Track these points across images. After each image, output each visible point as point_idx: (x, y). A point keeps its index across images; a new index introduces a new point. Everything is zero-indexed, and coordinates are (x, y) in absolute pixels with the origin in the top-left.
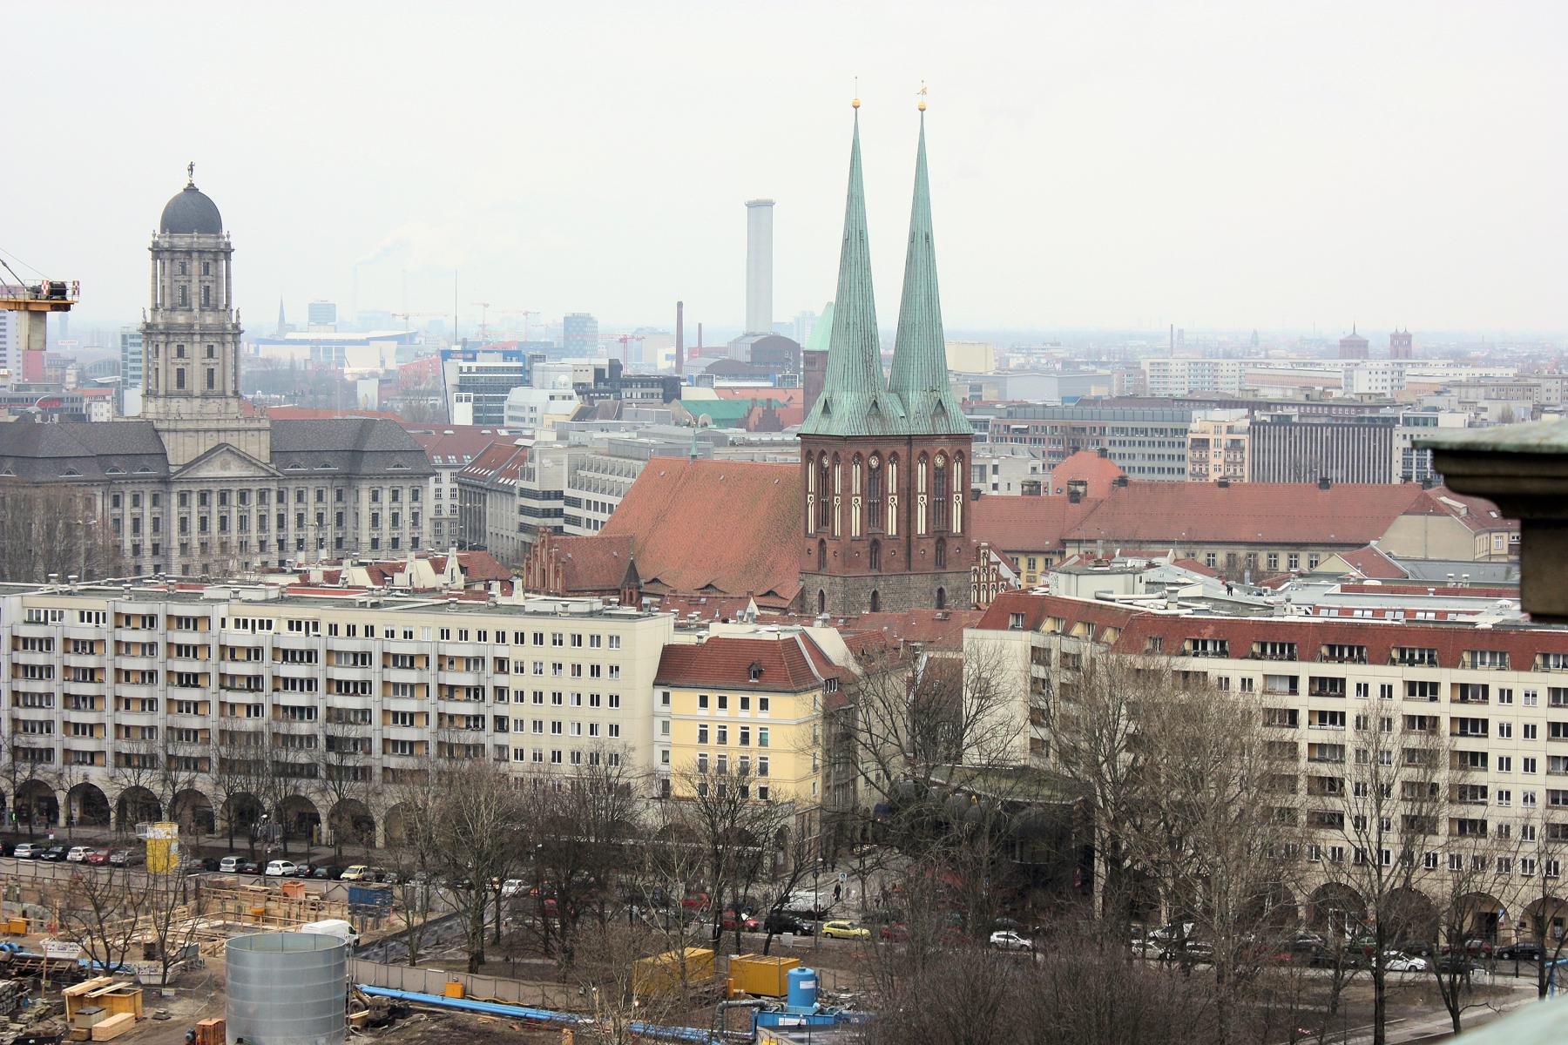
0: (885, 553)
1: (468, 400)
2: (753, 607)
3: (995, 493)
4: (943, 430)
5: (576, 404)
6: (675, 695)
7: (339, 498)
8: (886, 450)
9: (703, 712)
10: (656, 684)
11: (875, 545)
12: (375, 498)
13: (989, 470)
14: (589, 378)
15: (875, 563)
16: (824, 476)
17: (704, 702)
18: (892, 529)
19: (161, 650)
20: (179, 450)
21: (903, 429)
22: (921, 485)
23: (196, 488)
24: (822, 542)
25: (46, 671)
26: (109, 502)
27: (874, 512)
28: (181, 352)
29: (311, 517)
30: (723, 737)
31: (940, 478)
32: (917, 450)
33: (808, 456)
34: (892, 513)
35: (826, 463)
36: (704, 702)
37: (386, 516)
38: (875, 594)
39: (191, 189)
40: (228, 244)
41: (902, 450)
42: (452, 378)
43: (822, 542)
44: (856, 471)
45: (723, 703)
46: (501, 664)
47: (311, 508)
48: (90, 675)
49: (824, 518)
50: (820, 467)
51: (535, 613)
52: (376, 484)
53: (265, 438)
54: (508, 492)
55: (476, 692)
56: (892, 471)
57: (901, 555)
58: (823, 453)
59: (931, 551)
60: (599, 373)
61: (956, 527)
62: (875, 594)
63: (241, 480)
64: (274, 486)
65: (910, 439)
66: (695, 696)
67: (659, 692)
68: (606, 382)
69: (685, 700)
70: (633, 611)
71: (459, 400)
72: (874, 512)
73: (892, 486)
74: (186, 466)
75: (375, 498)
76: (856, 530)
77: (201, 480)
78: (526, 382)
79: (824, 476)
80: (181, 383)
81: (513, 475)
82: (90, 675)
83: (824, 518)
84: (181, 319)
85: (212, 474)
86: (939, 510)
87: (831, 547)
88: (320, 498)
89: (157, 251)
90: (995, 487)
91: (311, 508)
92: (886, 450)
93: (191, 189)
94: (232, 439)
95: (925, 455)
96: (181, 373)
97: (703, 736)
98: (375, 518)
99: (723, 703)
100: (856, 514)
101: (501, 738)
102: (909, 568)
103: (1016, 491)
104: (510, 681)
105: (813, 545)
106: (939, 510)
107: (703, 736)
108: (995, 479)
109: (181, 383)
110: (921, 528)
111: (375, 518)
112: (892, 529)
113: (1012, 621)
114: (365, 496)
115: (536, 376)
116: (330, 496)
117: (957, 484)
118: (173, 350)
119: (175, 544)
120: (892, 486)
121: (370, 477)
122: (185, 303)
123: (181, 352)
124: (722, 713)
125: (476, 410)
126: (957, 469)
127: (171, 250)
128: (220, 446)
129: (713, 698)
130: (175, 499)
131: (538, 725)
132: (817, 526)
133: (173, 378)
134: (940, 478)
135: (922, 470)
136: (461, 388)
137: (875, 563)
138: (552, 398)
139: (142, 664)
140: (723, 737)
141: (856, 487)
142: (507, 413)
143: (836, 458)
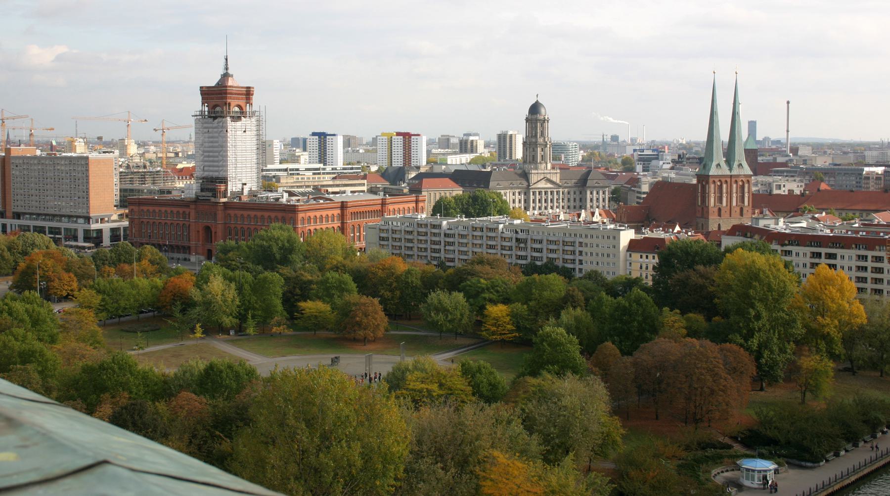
0: (723, 212)
1: (641, 164)
2: (677, 228)
3: (784, 193)
4: (743, 174)
5: (671, 165)
6: (633, 255)
7: (581, 193)
8: (723, 180)
9: (641, 260)
10: (627, 251)
11: (720, 210)
12: (591, 193)
13: (782, 186)
15: (720, 215)
17: (641, 257)
19: (485, 238)
20: (534, 178)
21: (728, 173)
22: (734, 190)
23: (537, 191)
24: (703, 208)
25: (453, 244)
26: (511, 194)
28: (534, 149)
29: (572, 199)
30: (647, 268)
32: (733, 180)
33: (698, 181)
34: (724, 200)
35: (704, 183)
36: (641, 257)
37: (595, 199)
38: (719, 225)
39: (537, 102)
40: (548, 118)
42: (636, 158)
43: (703, 208)
45: (647, 257)
47: (572, 196)
50: (702, 184)
51: (593, 229)
52: (592, 189)
53: (558, 175)
54: (634, 191)
55: (573, 252)
56: (724, 186)
57: (728, 212)
58: (703, 181)
59: (738, 211)
60: (679, 156)
62: (719, 225)
63: (551, 188)
64: (561, 190)
66: (639, 255)
67: (628, 253)
68: (682, 159)
69: (636, 256)
70: (623, 228)
71: (638, 164)
74: (535, 184)
75: (591, 193)
77: (539, 188)
78: (657, 159)
79: (703, 188)
80: (533, 160)
81: (635, 187)
84: (534, 140)
85: (542, 186)
88: (575, 193)
89: (527, 120)
90: (784, 191)
91: (572, 196)
93: (537, 102)
94: (548, 176)
95: (736, 182)
96: (533, 156)
97: (641, 267)
98: (591, 200)
99: (647, 257)
101: (581, 267)
102: (731, 216)
103: (786, 193)
104: (584, 249)
107: (641, 267)
108: (784, 189)
109: (533, 160)
111: (591, 200)
113: (737, 233)
114: (588, 193)
115: (660, 157)
116: (578, 193)
117: (746, 190)
118: (531, 150)
119: (531, 207)
120: (724, 190)
121: (589, 187)
122: (536, 136)
123: (534, 149)
124: (647, 260)
125: (643, 167)
126: (746, 186)
127: (531, 120)
128: (544, 178)
129: (644, 256)
130: (531, 193)
131: (591, 263)
132: (701, 203)
133: (531, 158)
136: (639, 161)
137: (720, 215)
138: (664, 163)
139: (479, 242)
140: (647, 268)
142: (650, 168)
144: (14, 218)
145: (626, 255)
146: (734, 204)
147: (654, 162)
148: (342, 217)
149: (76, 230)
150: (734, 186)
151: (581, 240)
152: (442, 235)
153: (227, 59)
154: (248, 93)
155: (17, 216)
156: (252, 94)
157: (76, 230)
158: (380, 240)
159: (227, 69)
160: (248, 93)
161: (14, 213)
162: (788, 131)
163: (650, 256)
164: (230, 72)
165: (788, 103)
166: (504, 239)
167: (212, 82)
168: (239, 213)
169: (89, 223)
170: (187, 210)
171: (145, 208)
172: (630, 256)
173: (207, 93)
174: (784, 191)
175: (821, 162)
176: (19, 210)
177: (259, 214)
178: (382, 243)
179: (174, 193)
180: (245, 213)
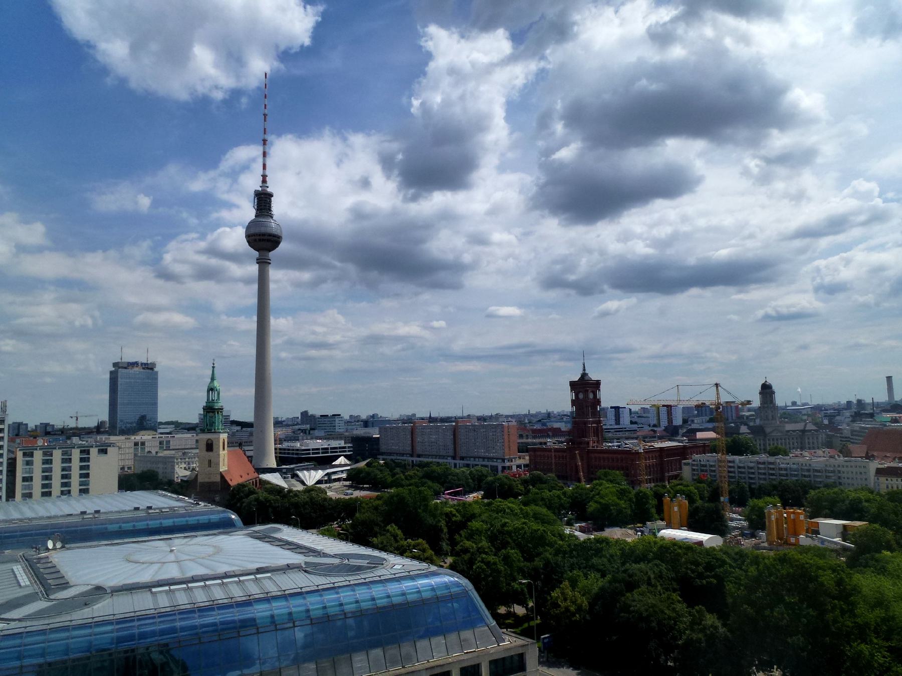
6: (880, 478)
17: (887, 480)
36: (887, 480)
46: (839, 472)
48: (753, 473)
66: (885, 479)
69: (882, 479)
70: (868, 460)
82: (753, 473)
129: (889, 479)
144: (461, 460)
145: (874, 479)
148: (661, 457)
149: (497, 467)
151: (839, 469)
152: (736, 467)
153: (584, 365)
154: (597, 384)
155: (462, 458)
156: (600, 384)
157: (497, 467)
158: (692, 471)
159: (584, 370)
160: (597, 384)
161: (461, 457)
163: (893, 479)
164: (587, 372)
166: (781, 469)
167: (576, 378)
168: (597, 455)
169: (504, 462)
170: (565, 454)
171: (538, 453)
172: (878, 479)
173: (573, 385)
176: (464, 455)
177: (611, 456)
178: (695, 473)
179: (548, 444)
180: (602, 455)
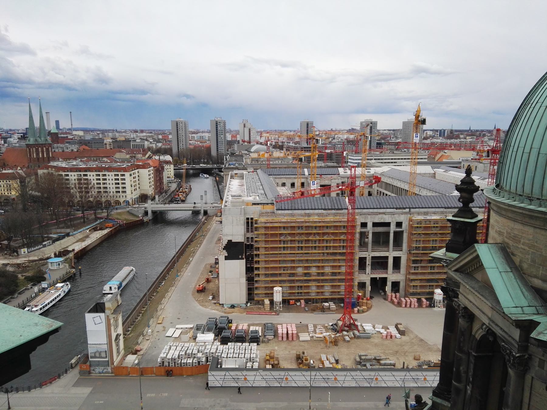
5: (18, 140)
14: (20, 137)
16: (30, 150)
18: (41, 156)
22: (45, 150)
27: (38, 154)
31: (47, 150)
33: (27, 147)
41: (41, 146)
44: (34, 149)
49: (30, 155)
56: (40, 149)
60: (21, 136)
61: (51, 156)
65: (42, 144)
72: (38, 154)
73: (40, 150)
76: (35, 157)
79: (30, 150)
83: (30, 155)
86: (48, 154)
87: (32, 159)
92: (38, 146)
100: (35, 155)
105: (29, 159)
106: (48, 154)
110: (45, 156)
112: (41, 156)
120: (40, 150)
126: (50, 148)
134: (47, 150)
135: (44, 148)
141: (34, 151)
143: (31, 147)
146: (45, 156)
147: (9, 139)
150: (44, 148)
162: (72, 125)
165: (71, 112)
174: (69, 150)
175: (88, 137)
